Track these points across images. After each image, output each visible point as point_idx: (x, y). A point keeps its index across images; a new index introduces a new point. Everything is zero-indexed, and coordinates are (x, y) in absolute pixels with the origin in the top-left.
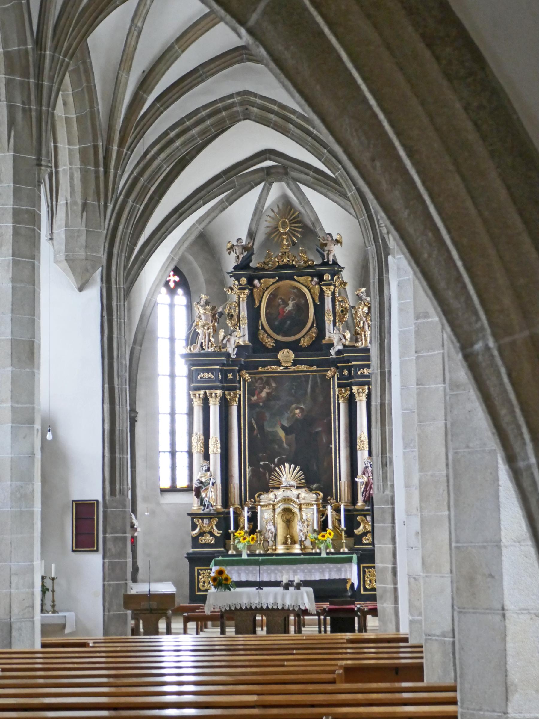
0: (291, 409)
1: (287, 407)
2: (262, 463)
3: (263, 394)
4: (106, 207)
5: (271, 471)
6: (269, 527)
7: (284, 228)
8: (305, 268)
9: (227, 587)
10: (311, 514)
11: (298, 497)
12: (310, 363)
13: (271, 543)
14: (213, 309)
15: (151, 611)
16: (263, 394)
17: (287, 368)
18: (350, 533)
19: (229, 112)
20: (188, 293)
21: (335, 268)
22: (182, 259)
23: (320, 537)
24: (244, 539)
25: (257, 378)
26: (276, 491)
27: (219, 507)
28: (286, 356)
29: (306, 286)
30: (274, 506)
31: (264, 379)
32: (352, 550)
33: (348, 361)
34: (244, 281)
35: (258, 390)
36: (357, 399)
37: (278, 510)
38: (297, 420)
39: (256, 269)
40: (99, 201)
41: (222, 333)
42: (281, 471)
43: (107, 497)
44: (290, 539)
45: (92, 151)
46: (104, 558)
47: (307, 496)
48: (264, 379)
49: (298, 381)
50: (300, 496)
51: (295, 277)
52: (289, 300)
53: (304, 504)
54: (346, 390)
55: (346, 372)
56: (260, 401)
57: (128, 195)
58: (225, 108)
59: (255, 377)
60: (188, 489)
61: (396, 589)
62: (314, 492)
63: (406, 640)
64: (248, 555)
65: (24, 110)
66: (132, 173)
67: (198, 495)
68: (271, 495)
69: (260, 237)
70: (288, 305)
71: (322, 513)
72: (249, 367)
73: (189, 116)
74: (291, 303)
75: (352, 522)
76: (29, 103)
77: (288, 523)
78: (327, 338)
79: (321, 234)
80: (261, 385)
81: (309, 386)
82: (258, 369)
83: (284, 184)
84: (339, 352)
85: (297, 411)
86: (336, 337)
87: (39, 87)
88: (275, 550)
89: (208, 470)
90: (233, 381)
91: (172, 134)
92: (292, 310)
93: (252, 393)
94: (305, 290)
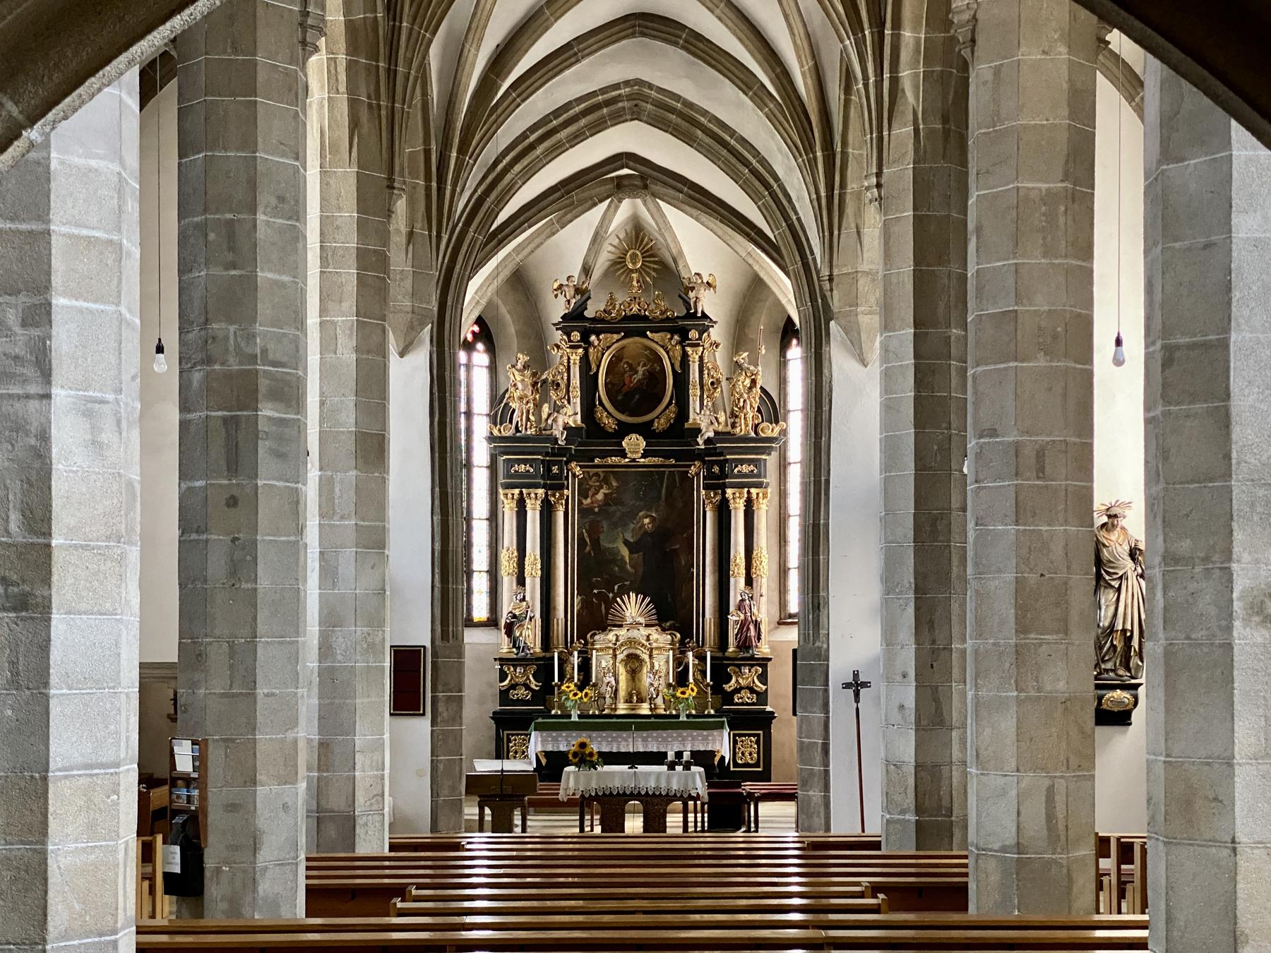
1: (632, 515)
3: (600, 496)
4: (439, 237)
5: (610, 604)
6: (607, 680)
7: (634, 264)
8: (662, 321)
9: (593, 766)
10: (663, 662)
11: (648, 639)
12: (666, 455)
13: (608, 701)
14: (534, 375)
15: (503, 797)
16: (600, 496)
17: (634, 460)
18: (717, 689)
19: (613, 108)
20: (491, 350)
21: (703, 322)
22: (490, 305)
23: (678, 694)
24: (575, 695)
26: (616, 631)
27: (538, 650)
28: (634, 444)
30: (614, 650)
32: (720, 712)
33: (721, 454)
34: (576, 336)
36: (732, 506)
37: (620, 657)
38: (646, 532)
39: (593, 320)
40: (430, 230)
41: (546, 409)
43: (438, 642)
44: (636, 696)
45: (422, 158)
46: (433, 723)
47: (660, 639)
49: (649, 478)
53: (657, 648)
54: (716, 494)
55: (716, 469)
57: (468, 223)
58: (608, 103)
60: (492, 622)
61: (827, 772)
63: (877, 845)
64: (579, 716)
65: (370, 105)
66: (475, 191)
67: (509, 632)
68: (611, 636)
69: (597, 273)
70: (637, 372)
71: (680, 662)
72: (584, 457)
73: (556, 113)
74: (641, 370)
75: (721, 675)
76: (378, 98)
77: (634, 674)
78: (691, 421)
79: (684, 274)
83: (639, 201)
84: (708, 441)
85: (647, 521)
86: (705, 420)
87: (392, 74)
88: (615, 709)
89: (524, 599)
90: (559, 476)
91: (533, 138)
93: (583, 493)
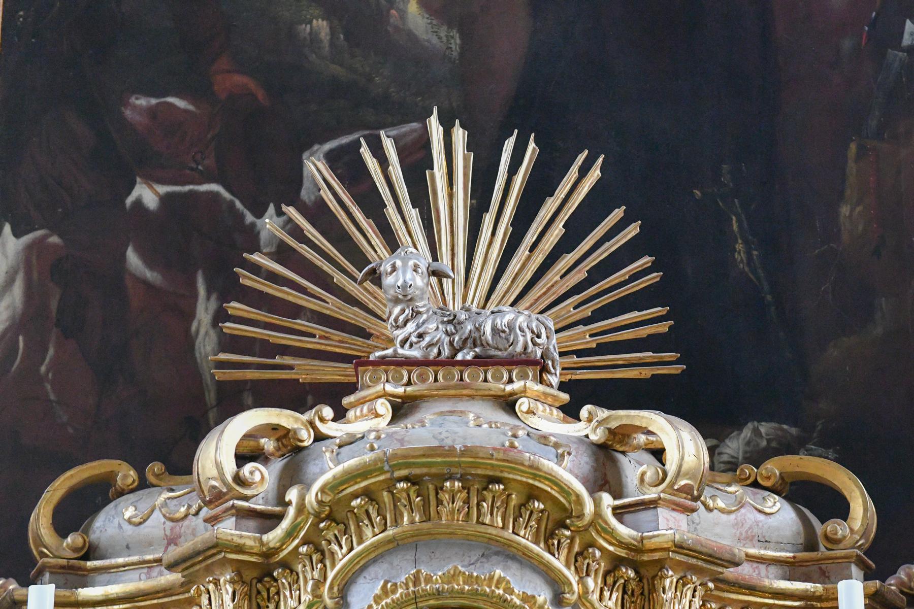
2: (147, 195)
42: (373, 206)
50: (635, 469)
62: (774, 467)
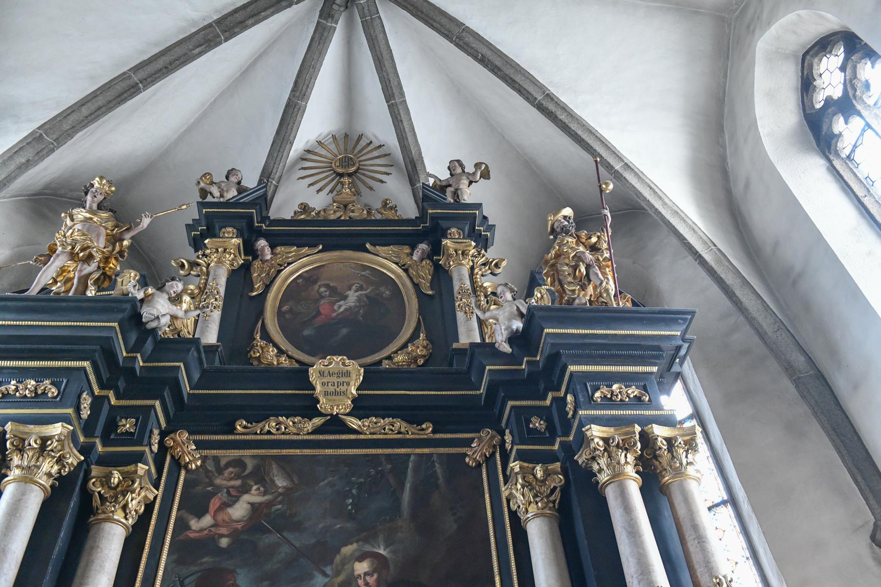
0: (338, 558)
3: (239, 511)
25: (223, 462)
29: (397, 264)
31: (250, 465)
35: (223, 496)
48: (250, 465)
51: (368, 246)
52: (350, 289)
56: (223, 531)
59: (216, 459)
70: (345, 298)
74: (353, 297)
80: (238, 483)
81: (408, 486)
82: (232, 430)
85: (362, 567)
92: (356, 307)
94: (392, 270)
